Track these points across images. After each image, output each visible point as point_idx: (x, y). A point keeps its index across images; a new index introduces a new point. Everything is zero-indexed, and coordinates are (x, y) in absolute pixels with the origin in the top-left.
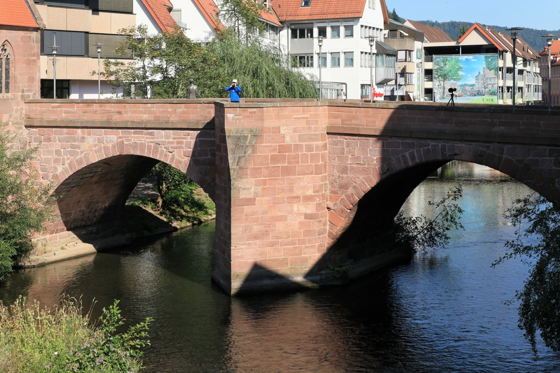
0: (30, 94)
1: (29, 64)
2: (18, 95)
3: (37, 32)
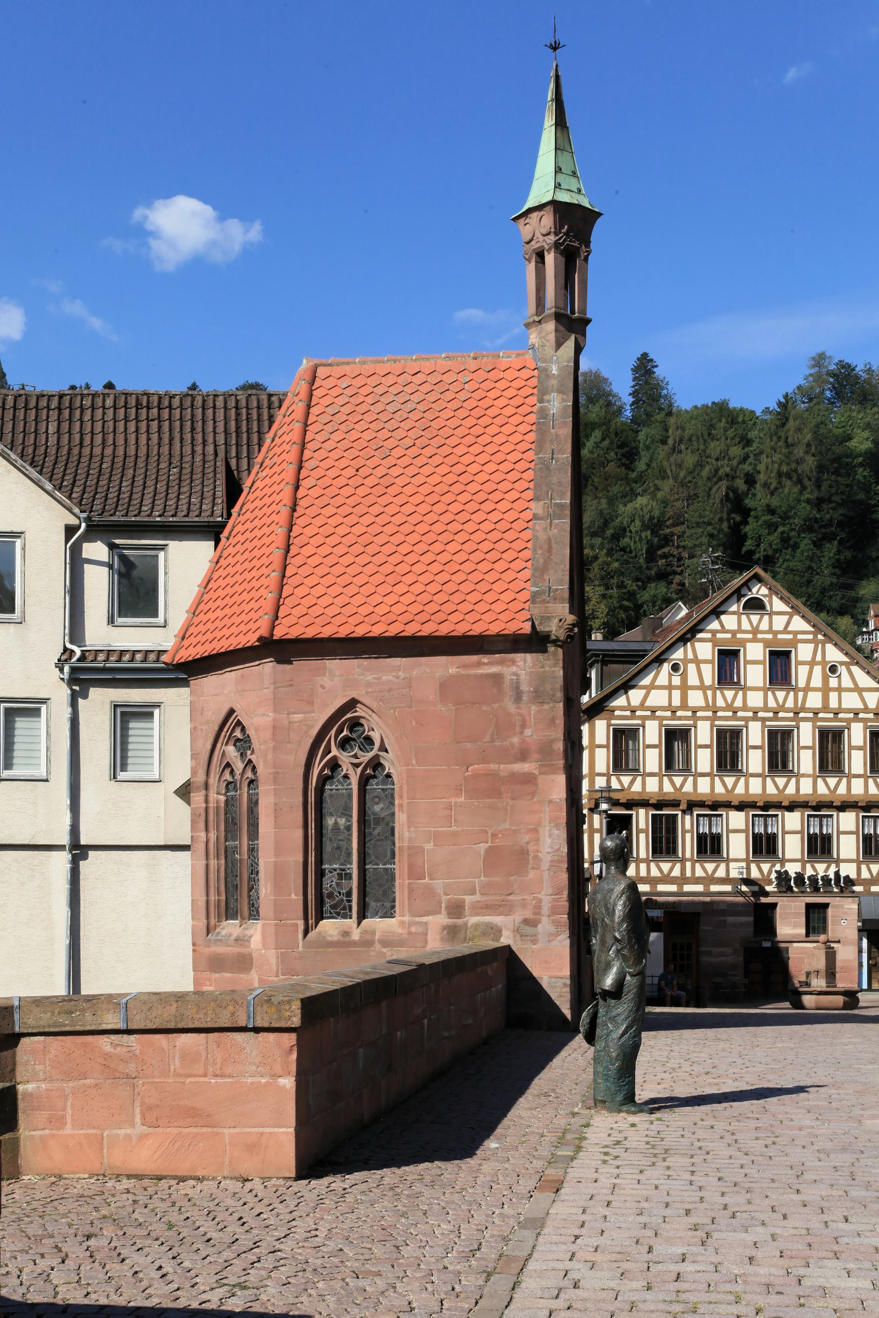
1: (495, 793)
3: (540, 656)
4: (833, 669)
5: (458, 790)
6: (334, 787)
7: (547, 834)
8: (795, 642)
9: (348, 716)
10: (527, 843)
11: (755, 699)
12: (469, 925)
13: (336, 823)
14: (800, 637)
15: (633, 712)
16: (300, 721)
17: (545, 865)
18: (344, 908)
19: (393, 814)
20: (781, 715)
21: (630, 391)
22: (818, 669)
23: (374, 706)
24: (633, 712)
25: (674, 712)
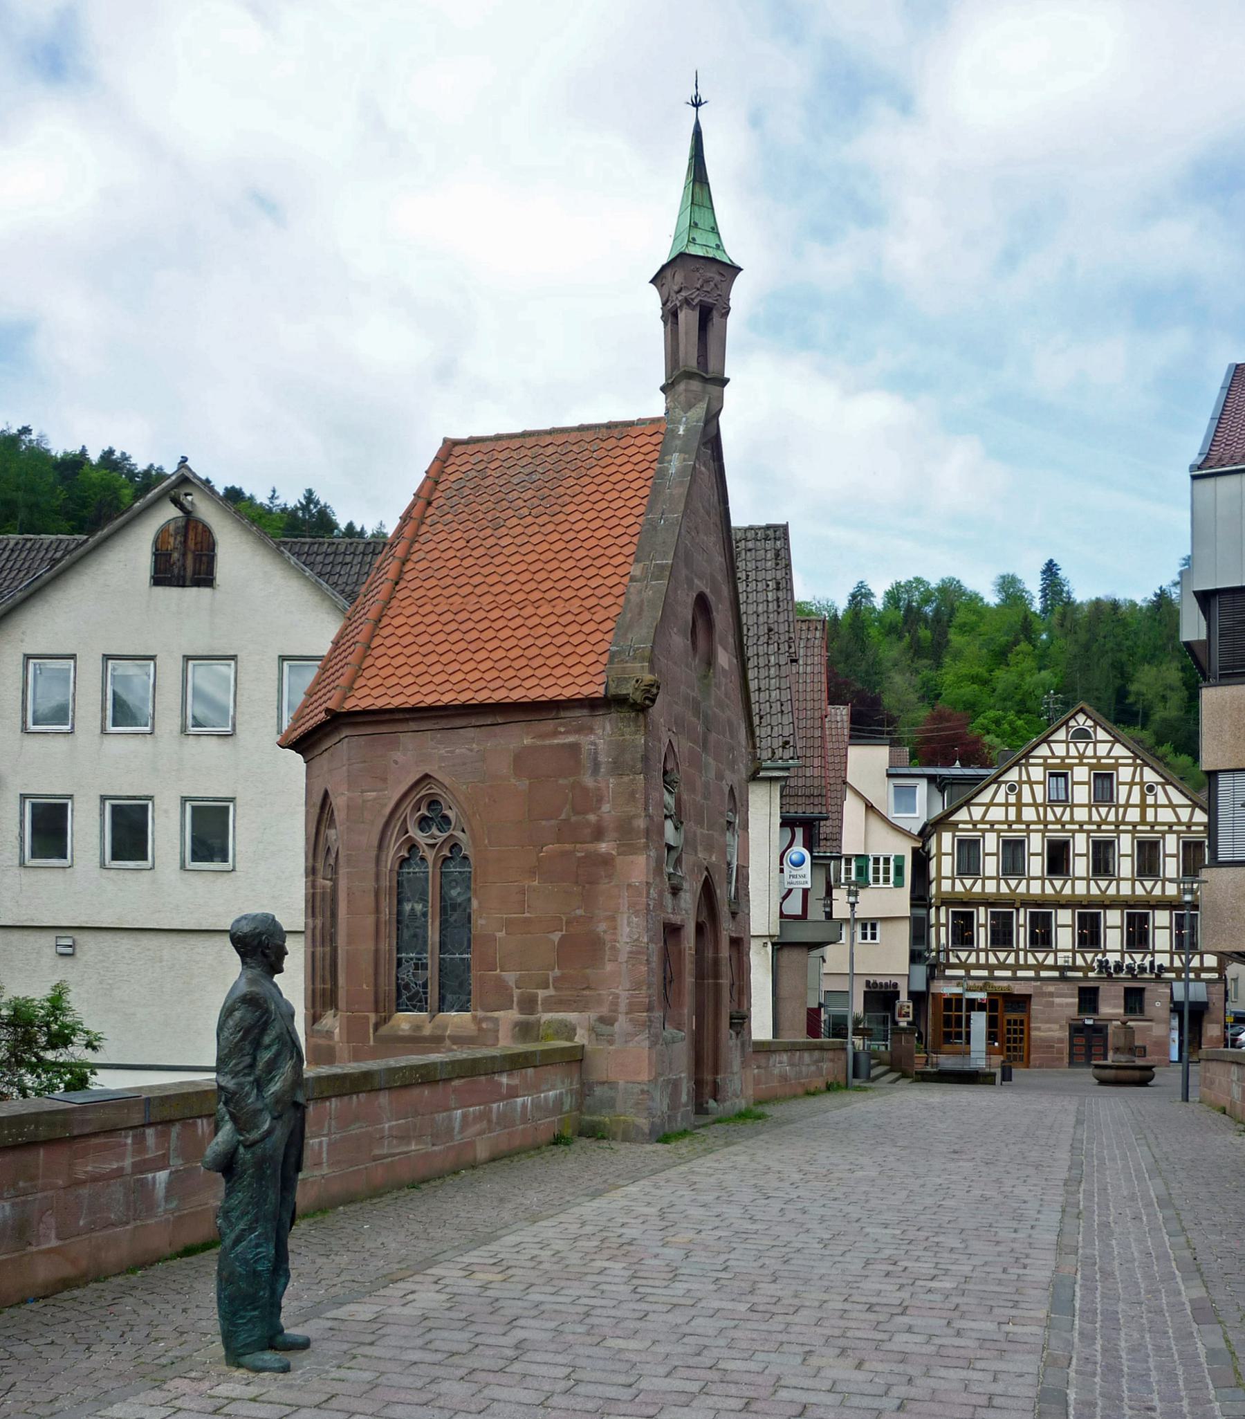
0: (571, 1017)
2: (496, 1020)
4: (1151, 789)
5: (532, 872)
6: (411, 870)
7: (625, 922)
8: (1116, 766)
9: (423, 793)
10: (605, 932)
11: (1081, 814)
12: (542, 1021)
13: (413, 909)
14: (1121, 761)
15: (975, 825)
16: (375, 799)
17: (623, 957)
18: (420, 1001)
19: (469, 900)
20: (1104, 827)
21: (1040, 588)
22: (1136, 789)
23: (447, 781)
24: (975, 825)
25: (1010, 826)
